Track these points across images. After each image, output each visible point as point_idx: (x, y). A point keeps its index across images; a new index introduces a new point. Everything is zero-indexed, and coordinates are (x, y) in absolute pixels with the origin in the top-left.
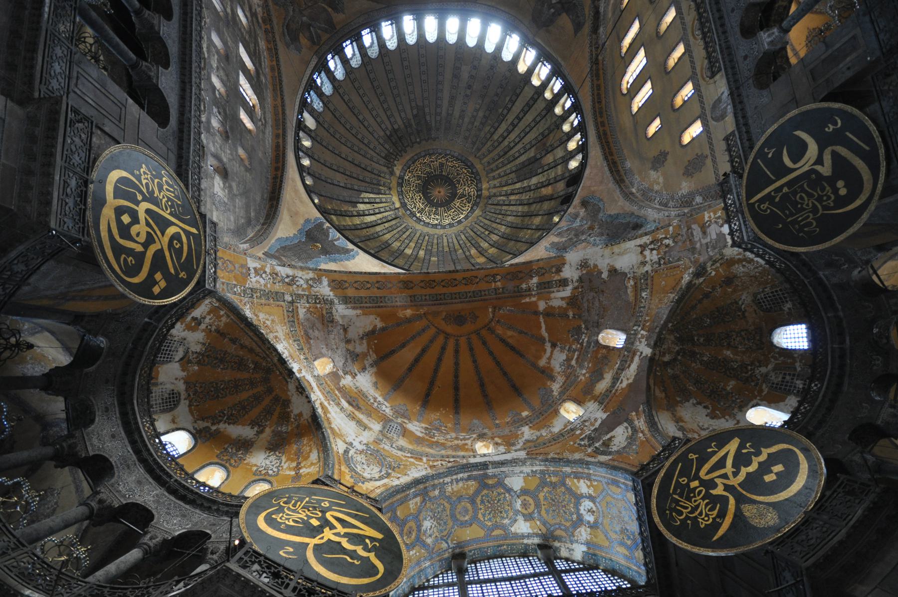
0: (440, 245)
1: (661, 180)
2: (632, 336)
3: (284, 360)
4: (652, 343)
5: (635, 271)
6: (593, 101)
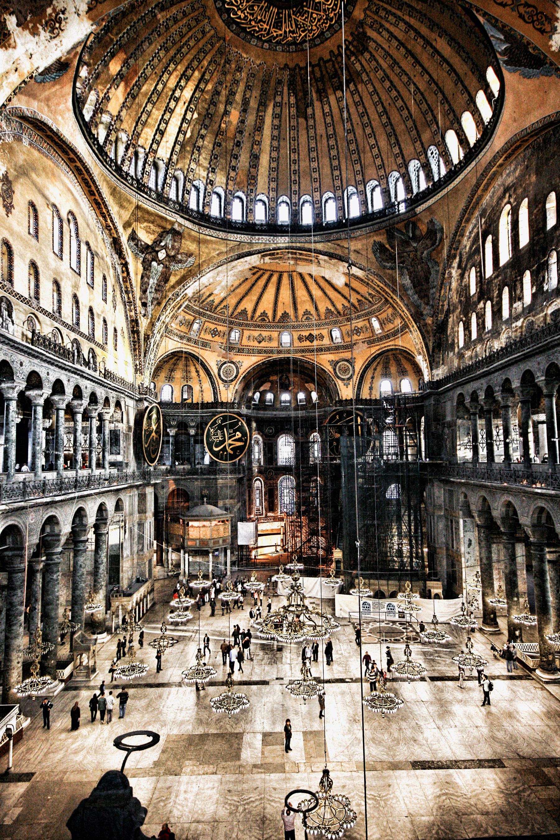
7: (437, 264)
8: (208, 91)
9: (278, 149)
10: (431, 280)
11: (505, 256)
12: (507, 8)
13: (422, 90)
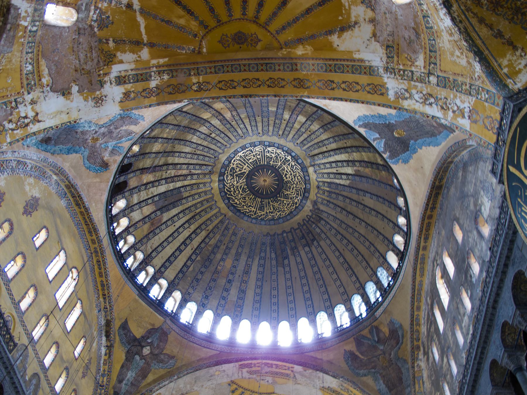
0: (266, 124)
1: (27, 188)
2: (37, 18)
3: (445, 6)
4: (12, 11)
5: (42, 94)
6: (105, 263)
7: (405, 361)
8: (210, 245)
9: (261, 287)
10: (404, 379)
11: (445, 297)
12: (360, 92)
13: (363, 234)
